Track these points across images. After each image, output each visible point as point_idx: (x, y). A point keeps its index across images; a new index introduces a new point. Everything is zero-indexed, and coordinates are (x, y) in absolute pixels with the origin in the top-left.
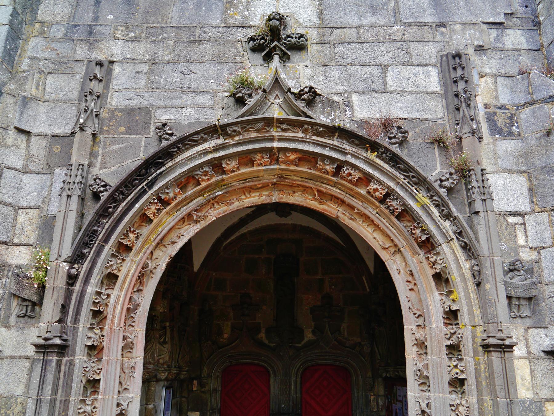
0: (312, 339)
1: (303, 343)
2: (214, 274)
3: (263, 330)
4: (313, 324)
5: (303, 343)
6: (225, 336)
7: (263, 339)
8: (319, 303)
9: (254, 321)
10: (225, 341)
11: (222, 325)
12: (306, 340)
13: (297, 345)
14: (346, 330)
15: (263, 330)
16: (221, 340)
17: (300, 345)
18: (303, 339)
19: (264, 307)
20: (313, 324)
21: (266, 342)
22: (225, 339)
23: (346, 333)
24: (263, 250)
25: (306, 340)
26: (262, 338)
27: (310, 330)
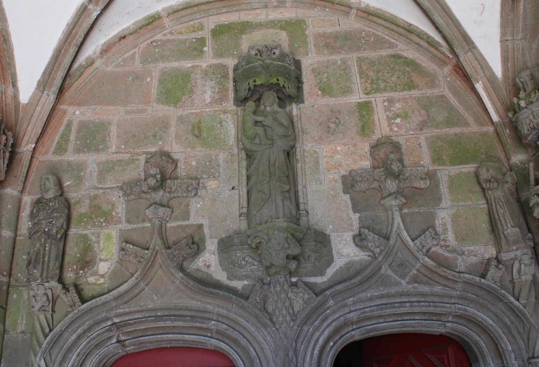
0: (357, 259)
1: (330, 272)
2: (77, 113)
3: (211, 245)
4: (355, 217)
5: (330, 272)
6: (103, 267)
7: (212, 268)
8: (367, 164)
9: (185, 223)
10: (102, 281)
11: (93, 238)
12: (338, 263)
13: (312, 280)
14: (449, 227)
15: (211, 245)
16: (91, 279)
17: (325, 279)
18: (330, 261)
19: (212, 184)
20: (355, 217)
21: (221, 276)
22: (102, 276)
23: (451, 237)
24: (205, 49)
25: (338, 263)
26: (209, 266)
27: (348, 236)
